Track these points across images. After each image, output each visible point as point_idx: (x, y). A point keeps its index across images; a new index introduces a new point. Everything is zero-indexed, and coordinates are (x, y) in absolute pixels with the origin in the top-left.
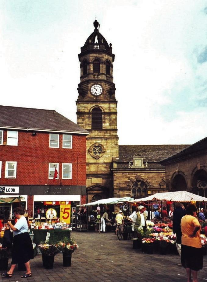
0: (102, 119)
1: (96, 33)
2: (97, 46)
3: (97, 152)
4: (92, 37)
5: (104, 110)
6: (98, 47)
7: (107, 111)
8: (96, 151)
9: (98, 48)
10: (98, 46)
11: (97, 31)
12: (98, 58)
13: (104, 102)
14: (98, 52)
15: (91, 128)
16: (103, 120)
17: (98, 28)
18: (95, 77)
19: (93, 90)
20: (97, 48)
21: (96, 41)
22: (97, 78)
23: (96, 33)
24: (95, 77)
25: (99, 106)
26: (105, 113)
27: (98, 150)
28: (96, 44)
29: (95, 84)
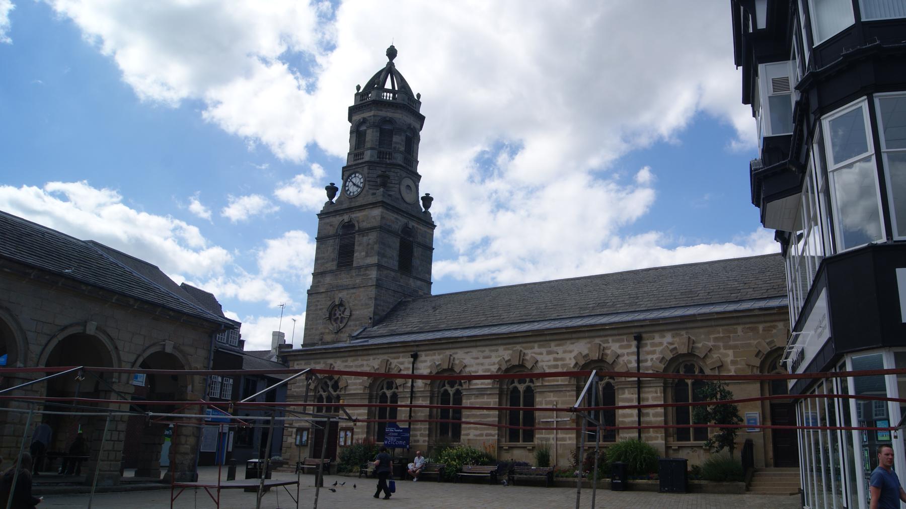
0: (354, 244)
1: (390, 70)
2: (388, 94)
4: (376, 82)
6: (390, 97)
7: (365, 225)
9: (391, 99)
10: (391, 95)
11: (392, 67)
13: (361, 208)
14: (365, 106)
15: (334, 268)
16: (356, 248)
21: (388, 85)
23: (390, 70)
28: (388, 91)
29: (352, 174)
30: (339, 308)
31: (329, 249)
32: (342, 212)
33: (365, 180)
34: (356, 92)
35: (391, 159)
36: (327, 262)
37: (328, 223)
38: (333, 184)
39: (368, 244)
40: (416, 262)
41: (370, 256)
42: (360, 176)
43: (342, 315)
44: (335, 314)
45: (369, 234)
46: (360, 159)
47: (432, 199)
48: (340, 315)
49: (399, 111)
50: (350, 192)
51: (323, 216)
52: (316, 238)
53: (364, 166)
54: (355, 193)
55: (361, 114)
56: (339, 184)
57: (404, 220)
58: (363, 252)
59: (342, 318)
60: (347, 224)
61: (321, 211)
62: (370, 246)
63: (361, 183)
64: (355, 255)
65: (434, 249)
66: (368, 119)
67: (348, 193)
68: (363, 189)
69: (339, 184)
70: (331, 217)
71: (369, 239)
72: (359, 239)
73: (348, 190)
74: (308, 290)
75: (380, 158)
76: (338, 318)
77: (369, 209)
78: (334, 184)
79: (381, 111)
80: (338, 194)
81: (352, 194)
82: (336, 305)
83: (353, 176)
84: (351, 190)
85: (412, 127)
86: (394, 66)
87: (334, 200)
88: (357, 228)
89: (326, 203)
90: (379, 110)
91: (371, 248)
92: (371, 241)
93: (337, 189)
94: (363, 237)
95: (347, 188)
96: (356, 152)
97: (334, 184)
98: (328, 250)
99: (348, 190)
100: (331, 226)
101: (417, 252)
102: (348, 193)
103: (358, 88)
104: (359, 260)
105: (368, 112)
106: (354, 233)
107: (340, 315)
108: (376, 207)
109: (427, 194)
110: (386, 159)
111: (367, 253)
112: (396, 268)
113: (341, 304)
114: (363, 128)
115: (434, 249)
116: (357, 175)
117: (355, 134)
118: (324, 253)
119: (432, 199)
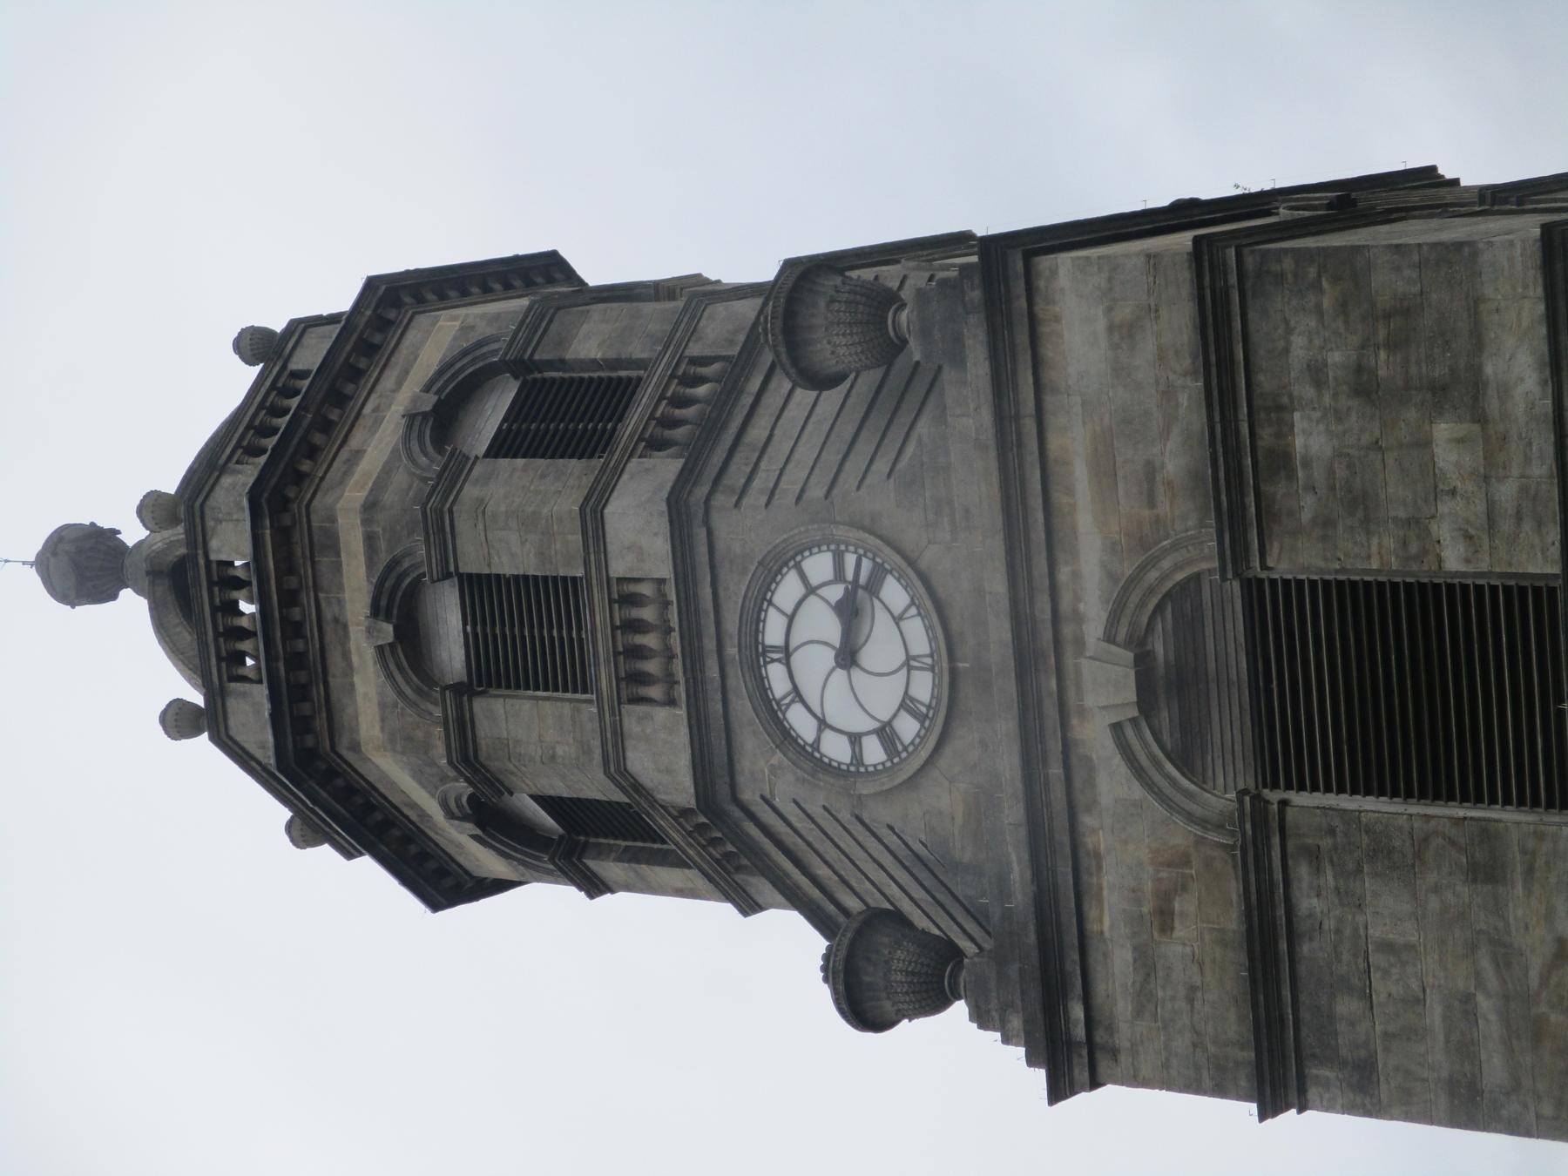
12: (376, 611)
19: (855, 739)
25: (1109, 637)
31: (1375, 932)
32: (1056, 770)
36: (1506, 956)
37: (1146, 962)
39: (1364, 386)
41: (1478, 341)
42: (788, 590)
45: (1265, 382)
49: (412, 337)
50: (907, 704)
51: (1077, 1012)
52: (1263, 1116)
53: (710, 533)
55: (346, 655)
58: (1425, 444)
60: (1165, 717)
61: (1031, 1061)
62: (1384, 364)
64: (1454, 560)
66: (384, 559)
67: (908, 728)
70: (1091, 913)
71: (1316, 373)
72: (1308, 507)
73: (886, 733)
77: (1050, 401)
79: (358, 454)
81: (923, 687)
89: (981, 1018)
90: (347, 473)
91: (1392, 345)
92: (1336, 357)
94: (1282, 461)
95: (874, 752)
96: (604, 678)
98: (1388, 947)
99: (886, 733)
100: (1165, 918)
102: (908, 728)
104: (1506, 492)
105: (338, 567)
106: (1253, 589)
108: (1033, 321)
111: (1439, 396)
116: (773, 633)
118: (1419, 1001)
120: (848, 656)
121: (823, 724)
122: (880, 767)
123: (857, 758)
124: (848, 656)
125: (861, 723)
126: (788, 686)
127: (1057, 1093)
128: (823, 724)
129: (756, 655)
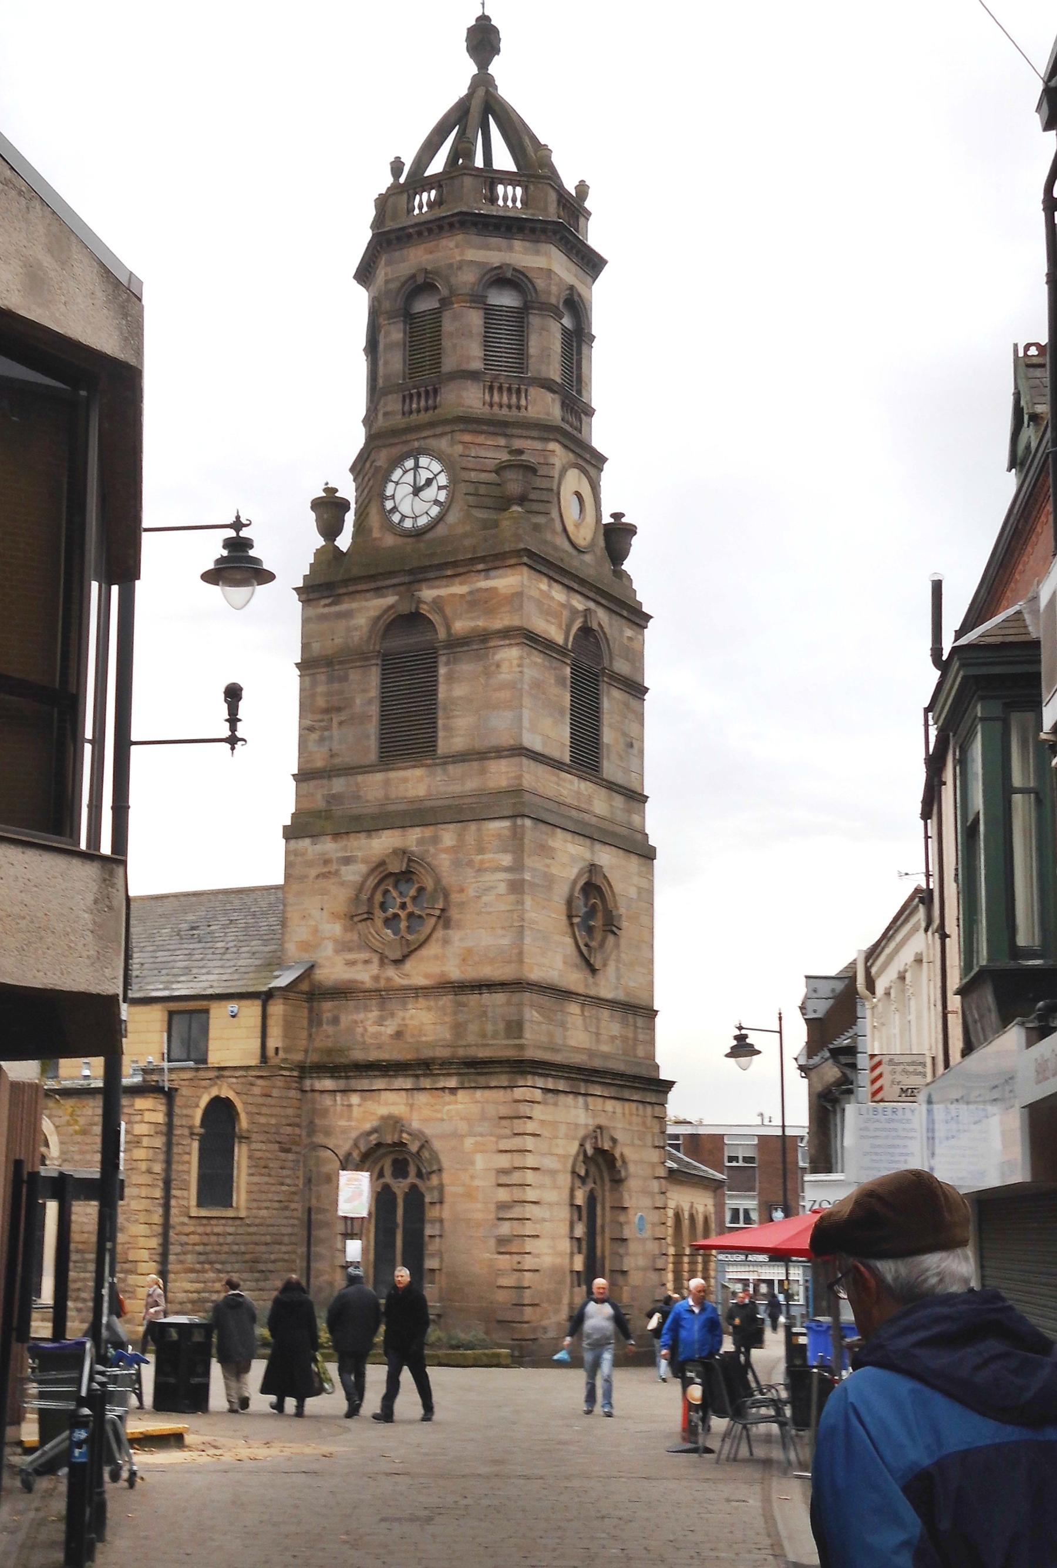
3: (403, 914)
5: (448, 628)
8: (403, 914)
17: (496, 68)
18: (414, 406)
19: (393, 497)
20: (510, 204)
22: (414, 416)
24: (505, 399)
26: (459, 644)
27: (407, 900)
30: (396, 886)
33: (453, 481)
34: (389, 180)
35: (526, 409)
38: (331, 491)
40: (608, 736)
42: (436, 467)
43: (410, 908)
44: (383, 906)
46: (427, 409)
47: (631, 530)
48: (403, 906)
50: (404, 517)
54: (422, 521)
56: (348, 490)
57: (579, 603)
59: (411, 915)
63: (440, 488)
65: (646, 690)
68: (445, 508)
69: (348, 490)
73: (395, 509)
74: (285, 828)
75: (491, 405)
76: (396, 916)
78: (336, 490)
80: (350, 518)
81: (408, 524)
82: (391, 874)
83: (410, 464)
84: (405, 508)
85: (576, 298)
86: (496, 88)
87: (344, 542)
88: (442, 634)
89: (318, 553)
93: (344, 505)
95: (389, 505)
97: (336, 490)
101: (611, 700)
102: (396, 518)
103: (397, 167)
107: (403, 906)
109: (617, 516)
110: (501, 406)
112: (567, 759)
113: (406, 876)
114: (425, 304)
115: (646, 690)
116: (424, 461)
117: (401, 326)
119: (631, 530)
120: (417, 491)
121: (397, 483)
122: (389, 505)
123: (387, 498)
124: (417, 491)
125: (398, 498)
126: (408, 468)
127: (295, 589)
128: (397, 483)
129: (416, 454)
